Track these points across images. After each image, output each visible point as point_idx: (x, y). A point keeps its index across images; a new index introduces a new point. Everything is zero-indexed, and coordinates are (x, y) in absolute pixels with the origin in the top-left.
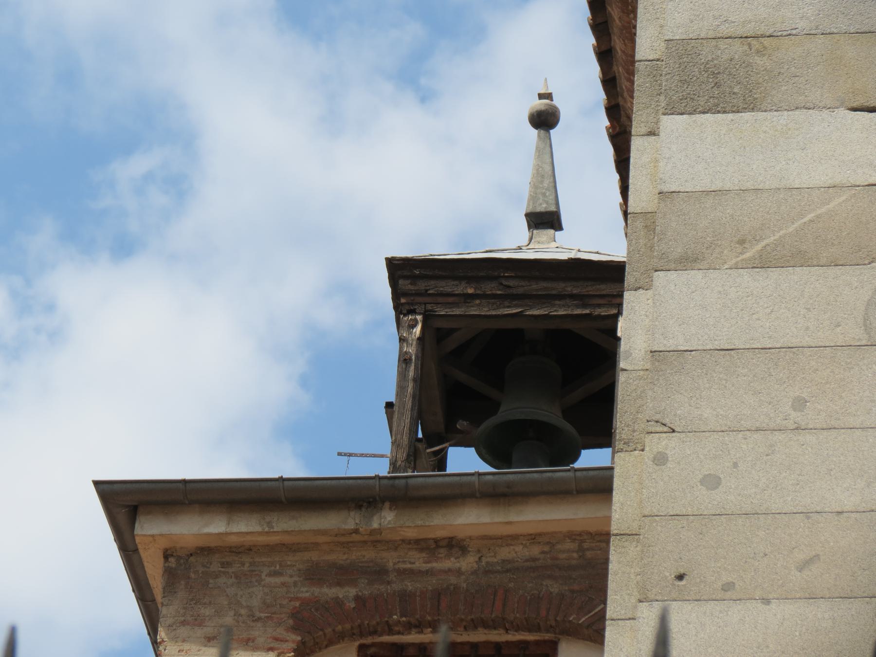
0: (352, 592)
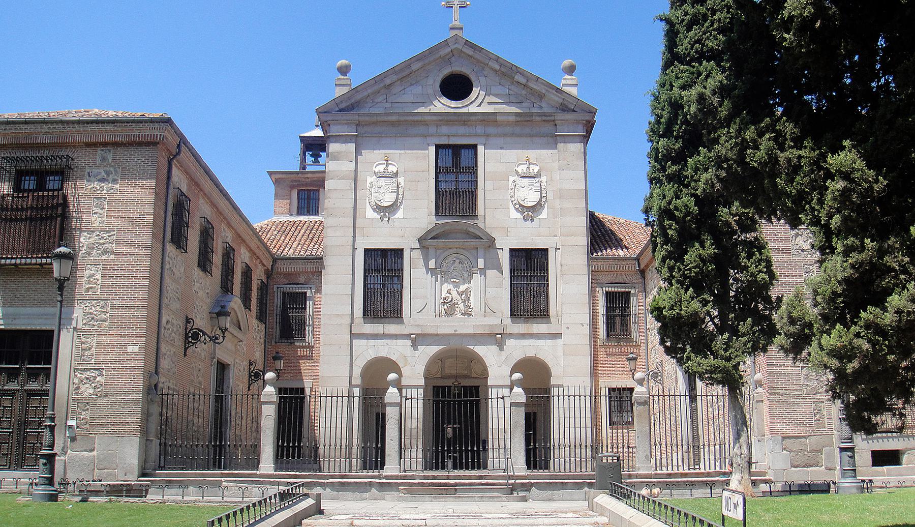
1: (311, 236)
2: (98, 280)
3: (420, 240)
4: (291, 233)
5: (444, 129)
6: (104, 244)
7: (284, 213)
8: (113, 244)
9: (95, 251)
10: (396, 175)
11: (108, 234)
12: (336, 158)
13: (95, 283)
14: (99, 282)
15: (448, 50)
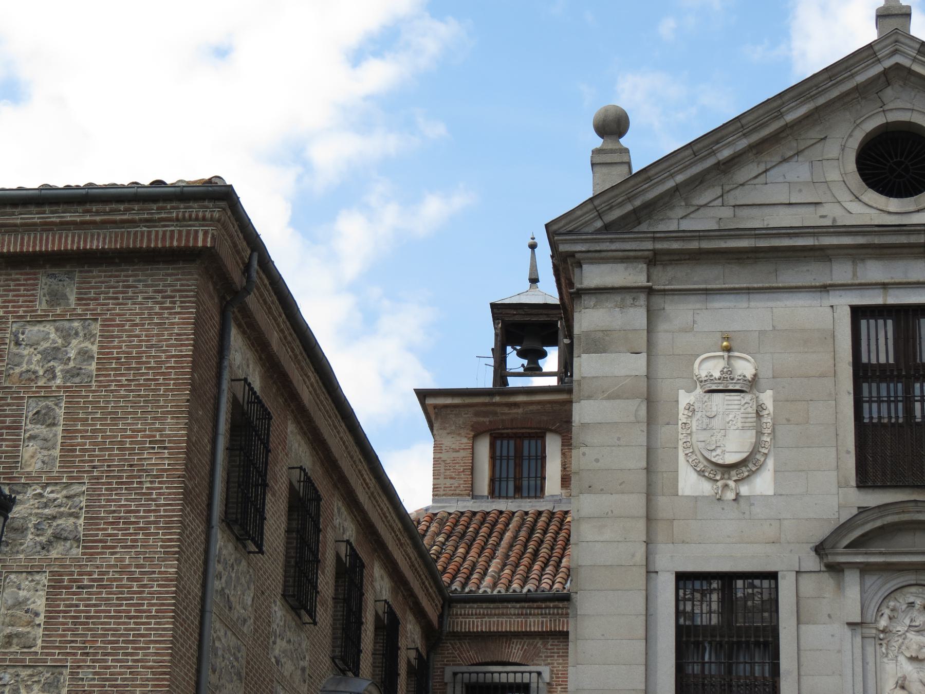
0: (488, 419)
1: (532, 546)
2: (37, 614)
3: (820, 549)
4: (479, 540)
5: (875, 271)
6: (54, 518)
7: (457, 492)
8: (78, 517)
9: (30, 536)
10: (752, 384)
11: (64, 492)
12: (598, 345)
13: (30, 623)
14: (41, 619)
15: (877, 69)
